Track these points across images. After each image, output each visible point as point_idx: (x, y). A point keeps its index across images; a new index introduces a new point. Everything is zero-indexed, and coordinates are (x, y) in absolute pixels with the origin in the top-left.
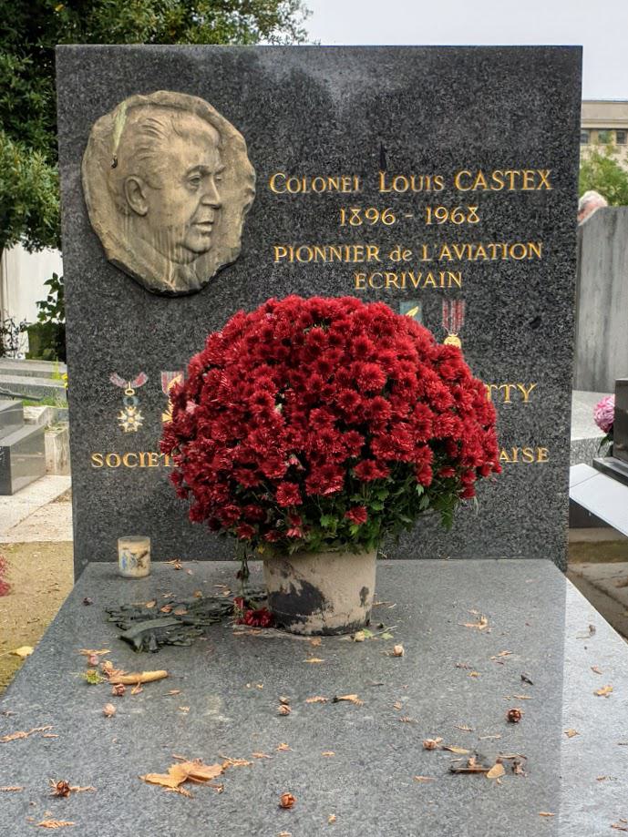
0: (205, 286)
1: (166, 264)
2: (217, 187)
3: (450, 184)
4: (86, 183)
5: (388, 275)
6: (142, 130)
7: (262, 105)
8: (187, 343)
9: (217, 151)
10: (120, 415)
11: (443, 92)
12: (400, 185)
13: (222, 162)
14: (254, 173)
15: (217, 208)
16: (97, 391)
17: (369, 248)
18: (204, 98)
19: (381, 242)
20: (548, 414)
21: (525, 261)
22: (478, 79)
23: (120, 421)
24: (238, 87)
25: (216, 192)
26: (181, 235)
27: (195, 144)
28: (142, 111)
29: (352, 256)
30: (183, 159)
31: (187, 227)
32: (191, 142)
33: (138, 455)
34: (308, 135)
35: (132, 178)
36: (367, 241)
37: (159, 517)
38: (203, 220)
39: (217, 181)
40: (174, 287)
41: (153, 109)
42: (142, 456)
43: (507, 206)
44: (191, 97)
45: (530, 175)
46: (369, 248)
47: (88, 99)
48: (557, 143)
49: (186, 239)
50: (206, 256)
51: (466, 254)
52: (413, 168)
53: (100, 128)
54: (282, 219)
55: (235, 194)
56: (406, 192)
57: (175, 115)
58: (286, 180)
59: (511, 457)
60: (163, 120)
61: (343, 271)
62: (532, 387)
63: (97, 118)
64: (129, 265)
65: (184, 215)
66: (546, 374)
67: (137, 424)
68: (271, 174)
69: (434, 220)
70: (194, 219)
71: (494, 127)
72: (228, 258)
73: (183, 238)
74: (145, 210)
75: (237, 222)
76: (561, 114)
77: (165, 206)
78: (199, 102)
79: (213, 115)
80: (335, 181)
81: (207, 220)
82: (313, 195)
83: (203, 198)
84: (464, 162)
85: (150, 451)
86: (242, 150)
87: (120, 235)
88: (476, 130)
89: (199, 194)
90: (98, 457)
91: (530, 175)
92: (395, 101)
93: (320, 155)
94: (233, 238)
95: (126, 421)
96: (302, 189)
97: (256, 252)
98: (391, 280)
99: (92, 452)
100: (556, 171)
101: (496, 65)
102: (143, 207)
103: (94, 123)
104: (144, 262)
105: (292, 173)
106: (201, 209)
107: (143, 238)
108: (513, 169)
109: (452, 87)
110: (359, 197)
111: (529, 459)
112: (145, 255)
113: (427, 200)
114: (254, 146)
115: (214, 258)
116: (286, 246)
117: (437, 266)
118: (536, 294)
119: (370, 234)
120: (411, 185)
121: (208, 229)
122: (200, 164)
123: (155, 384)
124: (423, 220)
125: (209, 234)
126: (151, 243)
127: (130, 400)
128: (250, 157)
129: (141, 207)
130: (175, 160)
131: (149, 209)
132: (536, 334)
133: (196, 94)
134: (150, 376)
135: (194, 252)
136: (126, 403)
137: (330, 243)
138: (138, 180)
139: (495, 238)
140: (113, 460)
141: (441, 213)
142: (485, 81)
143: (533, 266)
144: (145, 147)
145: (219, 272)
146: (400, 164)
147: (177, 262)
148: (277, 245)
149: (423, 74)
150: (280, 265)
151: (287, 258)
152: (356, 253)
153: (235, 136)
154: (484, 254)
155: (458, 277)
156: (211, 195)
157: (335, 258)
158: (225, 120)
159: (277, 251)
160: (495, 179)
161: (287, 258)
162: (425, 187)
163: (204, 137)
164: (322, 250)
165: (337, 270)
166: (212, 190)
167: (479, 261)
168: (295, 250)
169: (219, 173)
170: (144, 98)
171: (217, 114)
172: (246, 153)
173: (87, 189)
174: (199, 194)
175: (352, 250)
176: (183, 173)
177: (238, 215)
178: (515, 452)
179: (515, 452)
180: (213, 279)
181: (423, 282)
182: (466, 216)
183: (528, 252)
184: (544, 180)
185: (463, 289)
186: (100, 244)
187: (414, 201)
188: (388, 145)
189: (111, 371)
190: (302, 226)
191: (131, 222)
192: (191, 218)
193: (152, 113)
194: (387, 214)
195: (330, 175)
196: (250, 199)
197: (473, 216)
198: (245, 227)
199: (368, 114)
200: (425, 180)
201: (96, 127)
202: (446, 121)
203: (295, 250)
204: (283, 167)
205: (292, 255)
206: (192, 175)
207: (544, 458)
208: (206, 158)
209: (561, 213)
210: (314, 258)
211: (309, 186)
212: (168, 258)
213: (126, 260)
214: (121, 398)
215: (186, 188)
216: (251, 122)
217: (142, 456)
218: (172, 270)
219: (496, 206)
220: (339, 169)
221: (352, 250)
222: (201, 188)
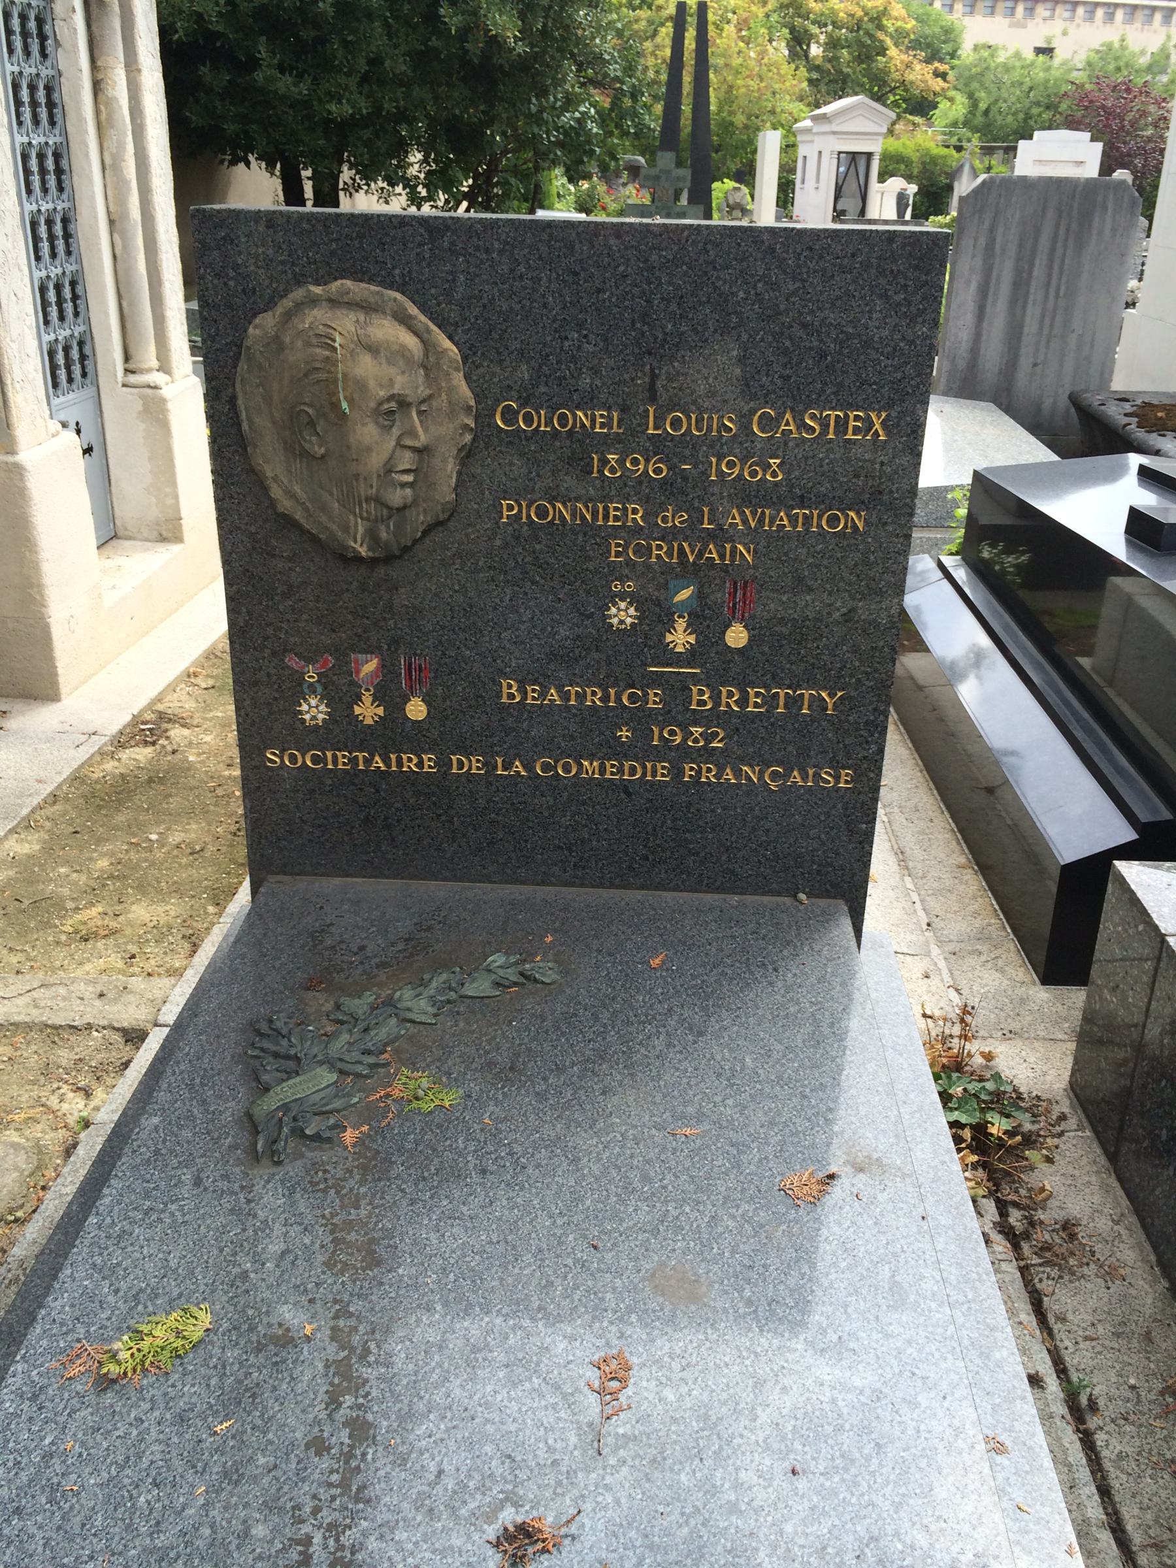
0: (406, 549)
1: (352, 522)
2: (421, 422)
3: (746, 428)
4: (242, 408)
5: (654, 544)
6: (314, 341)
7: (484, 306)
8: (384, 619)
9: (422, 372)
10: (300, 705)
11: (741, 294)
12: (676, 423)
13: (429, 386)
14: (472, 403)
15: (422, 452)
16: (269, 675)
17: (630, 507)
18: (403, 293)
19: (646, 501)
20: (858, 729)
21: (842, 535)
22: (794, 278)
23: (300, 712)
24: (450, 278)
25: (420, 430)
26: (371, 486)
27: (389, 362)
28: (315, 312)
29: (606, 517)
30: (372, 384)
31: (379, 476)
32: (383, 361)
33: (324, 754)
34: (548, 350)
35: (303, 407)
36: (627, 499)
37: (353, 828)
38: (401, 468)
39: (420, 413)
40: (363, 551)
41: (330, 308)
42: (329, 754)
43: (821, 460)
44: (385, 291)
45: (857, 418)
46: (630, 507)
47: (240, 288)
48: (899, 375)
49: (378, 491)
50: (407, 512)
51: (761, 521)
52: (694, 402)
53: (258, 332)
54: (511, 464)
55: (445, 433)
56: (682, 435)
57: (362, 318)
58: (518, 413)
59: (805, 778)
60: (346, 324)
61: (593, 536)
62: (839, 694)
63: (255, 316)
64: (302, 521)
65: (375, 462)
66: (859, 680)
67: (321, 716)
68: (498, 402)
69: (720, 473)
70: (388, 467)
71: (811, 349)
72: (437, 515)
73: (374, 490)
74: (323, 450)
75: (450, 467)
76: (910, 335)
77: (348, 447)
78: (395, 300)
79: (415, 318)
80: (586, 415)
81: (407, 467)
82: (555, 434)
83: (400, 437)
84: (766, 395)
85: (340, 751)
86: (457, 369)
87: (290, 481)
88: (786, 352)
89: (396, 432)
90: (274, 754)
91: (857, 418)
92: (673, 307)
93: (565, 378)
94: (445, 491)
95: (308, 712)
96: (539, 425)
97: (476, 506)
98: (659, 551)
99: (266, 748)
100: (894, 414)
101: (821, 257)
102: (320, 447)
103: (250, 323)
104: (324, 519)
105: (524, 402)
106: (398, 452)
107: (322, 488)
108: (833, 409)
109: (755, 287)
110: (618, 439)
111: (829, 782)
112: (324, 508)
113: (711, 446)
114: (473, 362)
115: (418, 514)
116: (516, 501)
117: (720, 536)
118: (854, 578)
119: (627, 488)
120: (690, 425)
121: (409, 478)
122: (396, 392)
123: (344, 668)
124: (706, 474)
125: (411, 485)
126: (331, 494)
127: (311, 685)
128: (467, 377)
129: (316, 448)
130: (362, 386)
131: (327, 451)
132: (850, 629)
133: (391, 286)
134: (337, 659)
135: (388, 507)
136: (306, 691)
137: (577, 499)
138: (310, 411)
139: (802, 502)
140: (293, 759)
141: (730, 465)
142: (805, 281)
143: (853, 541)
144: (318, 365)
145: (425, 533)
146: (676, 395)
147: (368, 520)
148: (505, 499)
149: (715, 268)
150: (507, 524)
151: (518, 516)
152: (612, 513)
153: (446, 350)
154: (786, 522)
155: (749, 552)
156: (412, 433)
157: (583, 518)
158: (430, 324)
159: (505, 507)
160: (808, 422)
161: (518, 516)
162: (710, 429)
163: (403, 352)
164: (566, 507)
165: (585, 534)
166: (413, 427)
167: (778, 531)
168: (529, 507)
169: (423, 401)
170: (317, 290)
171: (423, 318)
172: (461, 374)
173: (243, 415)
174: (396, 432)
175: (606, 509)
176: (373, 405)
177: (451, 459)
178: (811, 772)
179: (811, 772)
180: (416, 542)
181: (700, 555)
182: (765, 471)
183: (846, 524)
184: (877, 426)
185: (754, 567)
186: (265, 489)
187: (694, 447)
188: (660, 369)
189: (285, 651)
190: (538, 475)
191: (304, 465)
192: (385, 465)
193: (329, 315)
194: (655, 463)
195: (578, 407)
196: (468, 438)
197: (774, 472)
198: (459, 473)
199: (633, 322)
200: (710, 418)
201: (251, 330)
202: (745, 337)
203: (529, 507)
204: (514, 394)
205: (524, 511)
206: (386, 406)
207: (847, 782)
208: (404, 382)
209: (896, 472)
210: (554, 518)
211: (549, 422)
212: (355, 515)
213: (299, 516)
214: (300, 685)
215: (377, 423)
216: (469, 330)
217: (329, 754)
218: (361, 530)
219: (807, 458)
220: (592, 399)
221: (606, 509)
222: (398, 423)
